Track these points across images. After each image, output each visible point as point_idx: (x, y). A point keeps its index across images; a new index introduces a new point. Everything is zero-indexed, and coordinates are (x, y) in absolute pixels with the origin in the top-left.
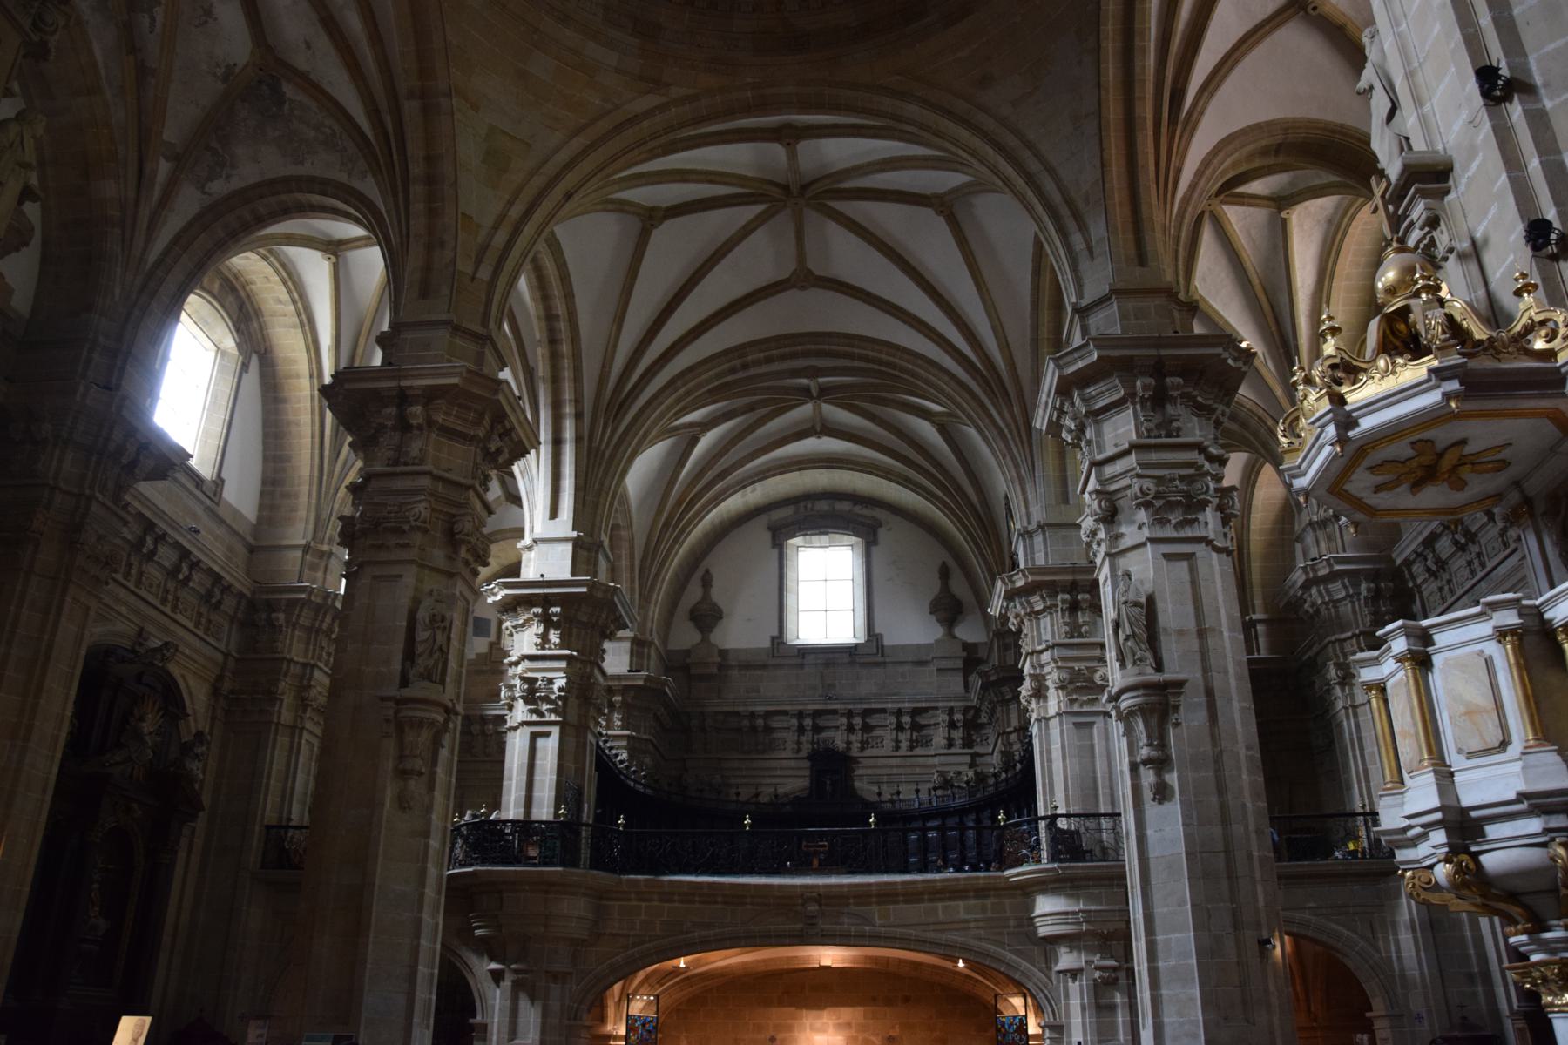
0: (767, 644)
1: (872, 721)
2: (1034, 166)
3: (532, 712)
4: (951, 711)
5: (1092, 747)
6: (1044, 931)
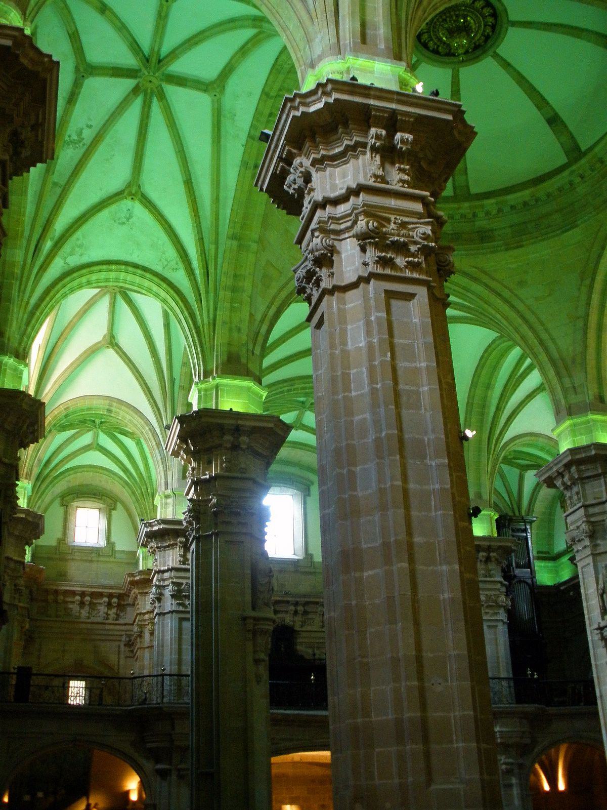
1: (309, 609)
2: (544, 336)
3: (179, 604)
5: (496, 639)
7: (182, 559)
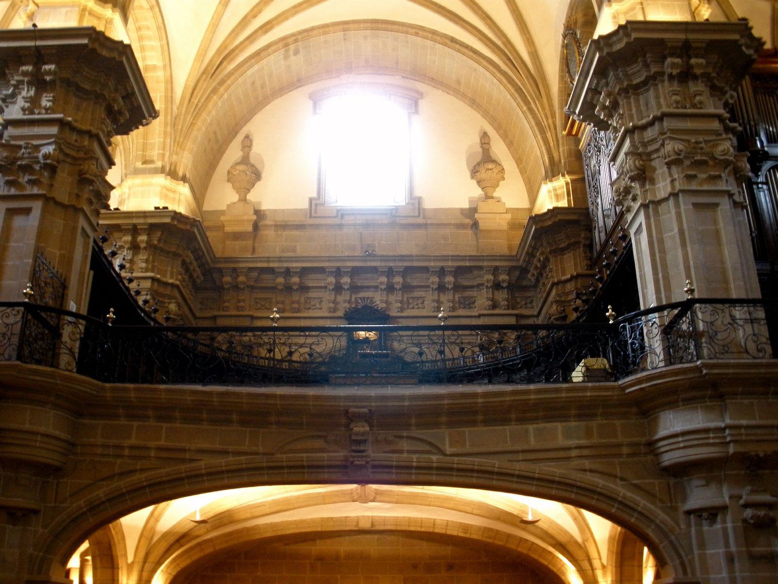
0: (305, 205)
4: (496, 270)
5: (717, 232)
6: (669, 458)
7: (27, 105)
